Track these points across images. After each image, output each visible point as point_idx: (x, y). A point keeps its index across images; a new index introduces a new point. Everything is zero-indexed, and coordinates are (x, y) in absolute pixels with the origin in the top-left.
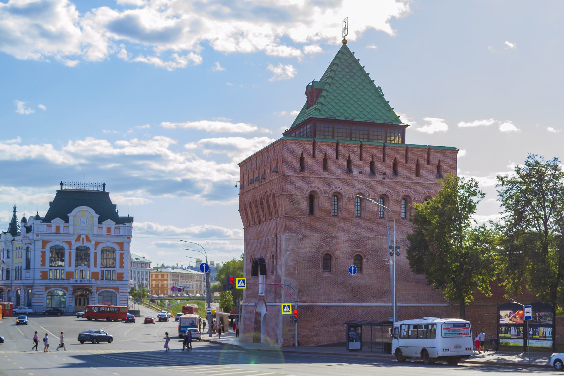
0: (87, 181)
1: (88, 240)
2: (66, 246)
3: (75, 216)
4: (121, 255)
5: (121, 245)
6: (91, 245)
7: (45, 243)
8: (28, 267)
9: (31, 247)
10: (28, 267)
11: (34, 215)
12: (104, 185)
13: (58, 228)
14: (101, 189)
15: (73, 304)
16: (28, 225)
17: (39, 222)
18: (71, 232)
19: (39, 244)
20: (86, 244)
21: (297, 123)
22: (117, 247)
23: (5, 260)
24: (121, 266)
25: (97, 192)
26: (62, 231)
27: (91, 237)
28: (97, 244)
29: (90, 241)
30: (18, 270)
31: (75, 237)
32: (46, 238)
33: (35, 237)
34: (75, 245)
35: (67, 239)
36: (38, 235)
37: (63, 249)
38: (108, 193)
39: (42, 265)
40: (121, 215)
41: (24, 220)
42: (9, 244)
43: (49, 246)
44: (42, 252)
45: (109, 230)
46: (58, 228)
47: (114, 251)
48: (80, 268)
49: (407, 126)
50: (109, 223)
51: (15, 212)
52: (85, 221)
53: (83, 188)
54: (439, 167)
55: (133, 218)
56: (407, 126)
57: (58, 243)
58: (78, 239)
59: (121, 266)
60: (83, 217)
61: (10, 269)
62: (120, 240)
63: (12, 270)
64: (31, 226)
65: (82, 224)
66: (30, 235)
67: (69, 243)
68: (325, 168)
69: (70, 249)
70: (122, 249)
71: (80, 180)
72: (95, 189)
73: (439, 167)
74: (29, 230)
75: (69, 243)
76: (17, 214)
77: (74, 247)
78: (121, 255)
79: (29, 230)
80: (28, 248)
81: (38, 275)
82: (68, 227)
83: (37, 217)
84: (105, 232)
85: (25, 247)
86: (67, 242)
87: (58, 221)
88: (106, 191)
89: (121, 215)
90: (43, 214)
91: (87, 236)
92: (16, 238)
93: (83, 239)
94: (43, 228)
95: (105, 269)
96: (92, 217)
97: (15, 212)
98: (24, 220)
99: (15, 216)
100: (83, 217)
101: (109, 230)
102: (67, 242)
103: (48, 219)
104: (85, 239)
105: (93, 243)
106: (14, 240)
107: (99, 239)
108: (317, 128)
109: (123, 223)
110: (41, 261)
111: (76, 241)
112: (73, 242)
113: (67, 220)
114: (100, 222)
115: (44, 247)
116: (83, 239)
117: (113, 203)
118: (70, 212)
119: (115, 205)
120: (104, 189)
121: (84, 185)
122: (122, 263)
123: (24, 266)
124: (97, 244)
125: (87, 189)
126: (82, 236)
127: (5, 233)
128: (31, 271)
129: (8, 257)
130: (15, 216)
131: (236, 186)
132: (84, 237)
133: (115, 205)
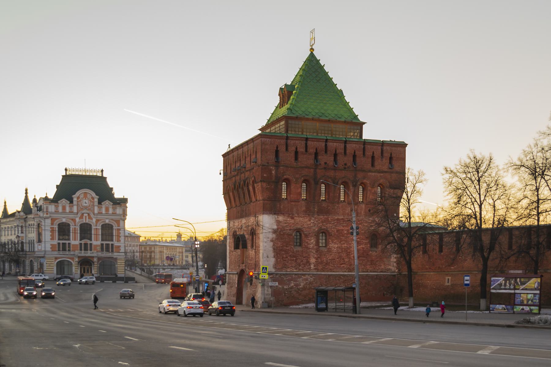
1: (90, 218)
3: (78, 198)
5: (118, 222)
7: (53, 220)
8: (40, 241)
9: (43, 224)
11: (44, 197)
12: (102, 171)
13: (64, 208)
14: (99, 174)
15: (79, 272)
16: (39, 205)
19: (49, 221)
21: (271, 121)
23: (19, 235)
26: (68, 209)
27: (92, 215)
28: (97, 221)
29: (92, 219)
30: (31, 243)
31: (79, 215)
32: (55, 216)
35: (72, 216)
36: (47, 214)
38: (106, 178)
39: (51, 239)
40: (117, 196)
41: (35, 200)
42: (23, 221)
44: (51, 228)
45: (107, 209)
46: (64, 208)
48: (83, 242)
49: (364, 123)
50: (107, 203)
51: (26, 193)
52: (87, 201)
53: (84, 174)
54: (391, 158)
55: (127, 199)
56: (364, 123)
57: (64, 220)
58: (81, 217)
59: (119, 241)
60: (85, 197)
61: (24, 241)
63: (26, 243)
64: (41, 206)
65: (86, 205)
68: (296, 158)
69: (75, 225)
70: (119, 226)
72: (95, 174)
73: (391, 158)
75: (74, 220)
76: (28, 195)
79: (40, 209)
80: (39, 224)
81: (48, 248)
82: (73, 206)
83: (46, 199)
84: (104, 211)
85: (36, 224)
86: (72, 220)
87: (64, 202)
88: (104, 176)
89: (117, 196)
90: (51, 196)
91: (88, 214)
92: (29, 216)
93: (86, 217)
94: (52, 208)
95: (105, 243)
96: (93, 198)
97: (26, 193)
98: (35, 200)
99: (26, 197)
100: (85, 197)
101: (107, 209)
102: (72, 220)
104: (87, 217)
105: (94, 220)
106: (27, 218)
107: (99, 217)
108: (290, 125)
109: (119, 204)
110: (51, 235)
111: (80, 218)
112: (77, 220)
113: (71, 202)
114: (100, 203)
115: (52, 224)
116: (86, 217)
117: (111, 186)
118: (74, 194)
119: (112, 189)
120: (102, 174)
121: (85, 171)
122: (119, 236)
123: (36, 239)
125: (88, 174)
126: (85, 215)
127: (19, 212)
129: (22, 233)
130: (26, 197)
131: (220, 174)
132: (87, 215)
133: (112, 189)
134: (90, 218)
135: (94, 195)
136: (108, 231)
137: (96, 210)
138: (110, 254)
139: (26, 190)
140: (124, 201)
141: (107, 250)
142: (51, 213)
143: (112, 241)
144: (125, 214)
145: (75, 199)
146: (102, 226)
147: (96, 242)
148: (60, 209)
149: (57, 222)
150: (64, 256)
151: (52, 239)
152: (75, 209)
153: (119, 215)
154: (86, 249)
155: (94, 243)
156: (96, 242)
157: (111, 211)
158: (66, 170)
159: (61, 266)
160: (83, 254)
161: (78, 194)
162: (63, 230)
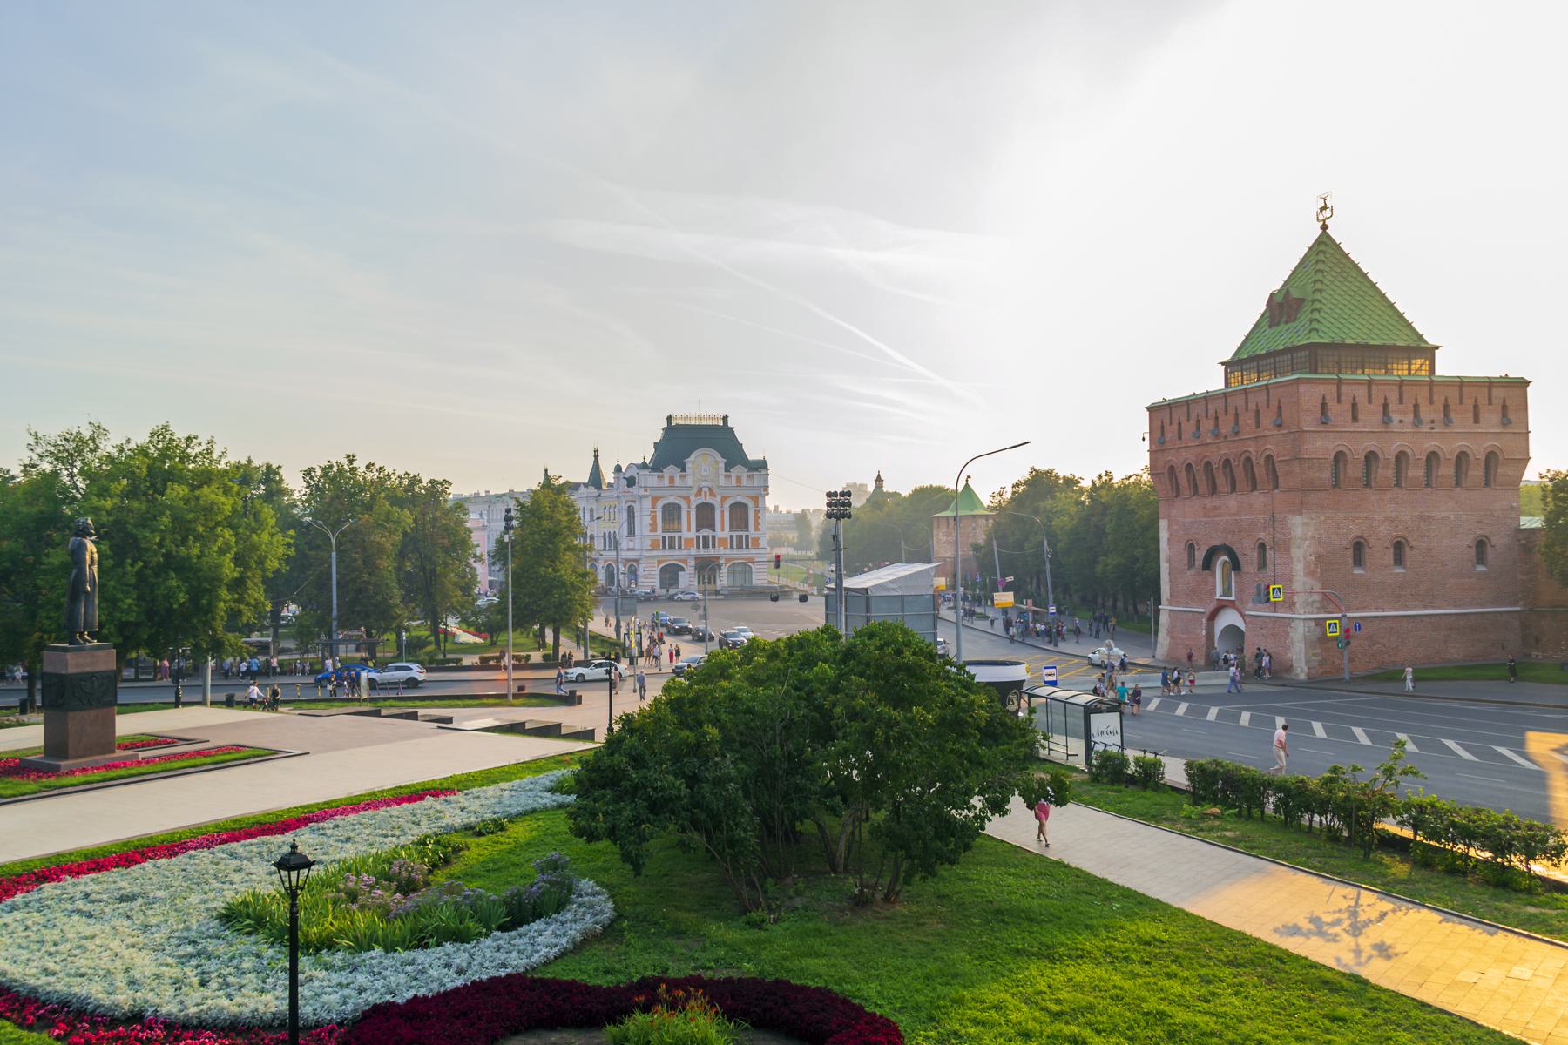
0: (704, 413)
1: (712, 494)
2: (683, 504)
4: (757, 512)
5: (756, 499)
6: (716, 501)
7: (655, 500)
8: (631, 533)
9: (636, 506)
10: (631, 533)
12: (725, 418)
13: (672, 479)
17: (646, 472)
18: (690, 482)
19: (647, 503)
20: (709, 500)
22: (750, 504)
24: (757, 529)
25: (716, 427)
26: (678, 482)
27: (715, 490)
28: (724, 499)
32: (657, 494)
33: (642, 492)
34: (695, 501)
35: (684, 493)
37: (679, 507)
43: (660, 504)
45: (739, 479)
46: (672, 479)
47: (745, 506)
50: (739, 470)
59: (757, 529)
62: (753, 493)
66: (634, 490)
67: (687, 499)
71: (694, 411)
74: (631, 482)
75: (687, 499)
77: (693, 506)
78: (757, 512)
81: (648, 542)
83: (644, 466)
84: (734, 483)
85: (625, 506)
87: (671, 470)
94: (651, 480)
101: (739, 479)
103: (657, 465)
105: (719, 498)
107: (727, 493)
112: (692, 498)
113: (684, 470)
114: (727, 470)
122: (757, 524)
124: (724, 499)
128: (637, 540)
134: (712, 494)
135: (719, 458)
136: (740, 515)
137: (722, 481)
138: (745, 551)
139: (596, 451)
140: (761, 466)
141: (740, 547)
142: (653, 488)
143: (746, 528)
144: (766, 488)
145: (688, 466)
146: (733, 506)
147: (723, 531)
148: (666, 482)
149: (660, 504)
150: (673, 557)
151: (653, 528)
152: (690, 482)
153: (758, 488)
154: (706, 546)
155: (719, 534)
156: (723, 531)
157: (745, 482)
158: (669, 418)
159: (670, 574)
160: (703, 552)
161: (692, 458)
162: (672, 512)
